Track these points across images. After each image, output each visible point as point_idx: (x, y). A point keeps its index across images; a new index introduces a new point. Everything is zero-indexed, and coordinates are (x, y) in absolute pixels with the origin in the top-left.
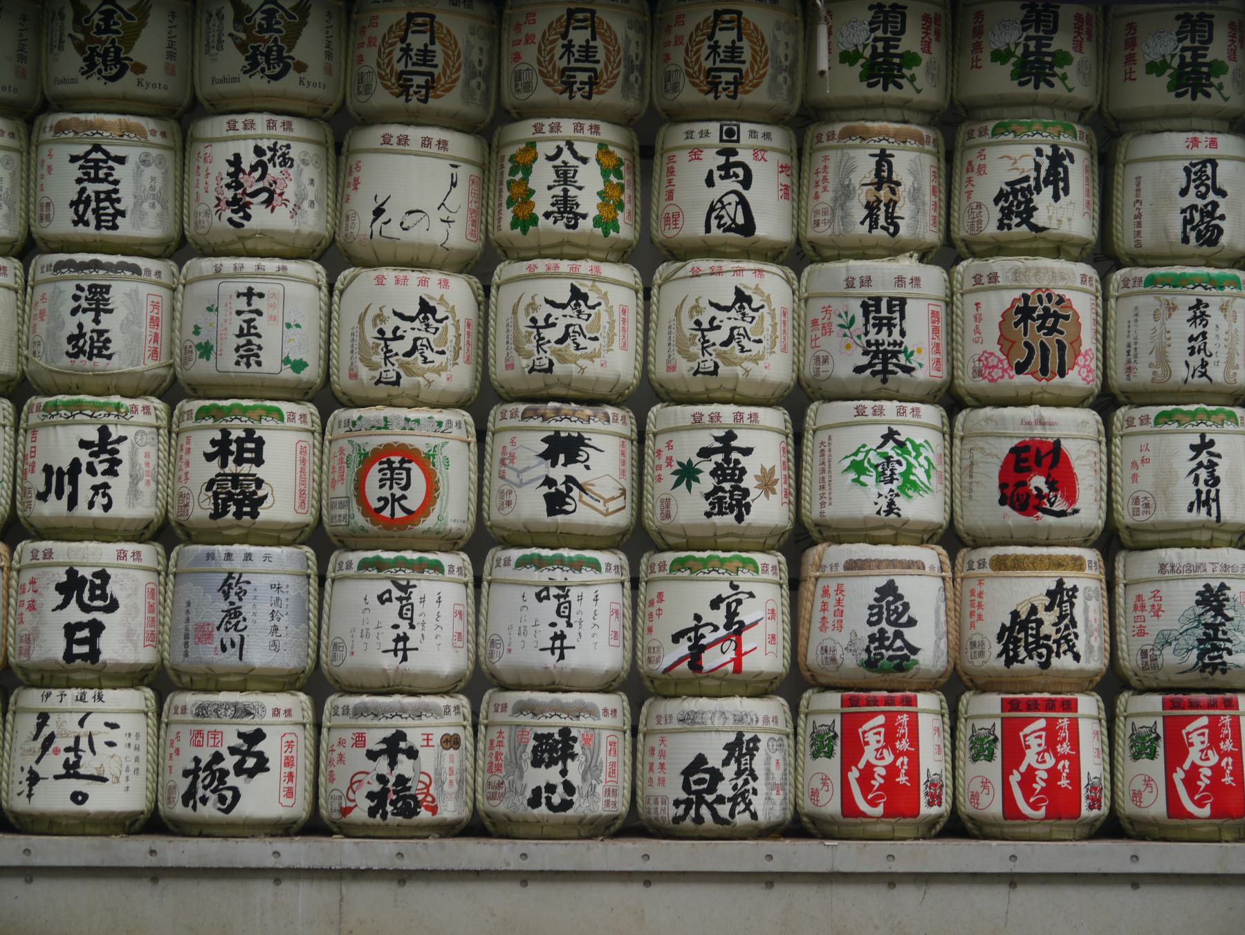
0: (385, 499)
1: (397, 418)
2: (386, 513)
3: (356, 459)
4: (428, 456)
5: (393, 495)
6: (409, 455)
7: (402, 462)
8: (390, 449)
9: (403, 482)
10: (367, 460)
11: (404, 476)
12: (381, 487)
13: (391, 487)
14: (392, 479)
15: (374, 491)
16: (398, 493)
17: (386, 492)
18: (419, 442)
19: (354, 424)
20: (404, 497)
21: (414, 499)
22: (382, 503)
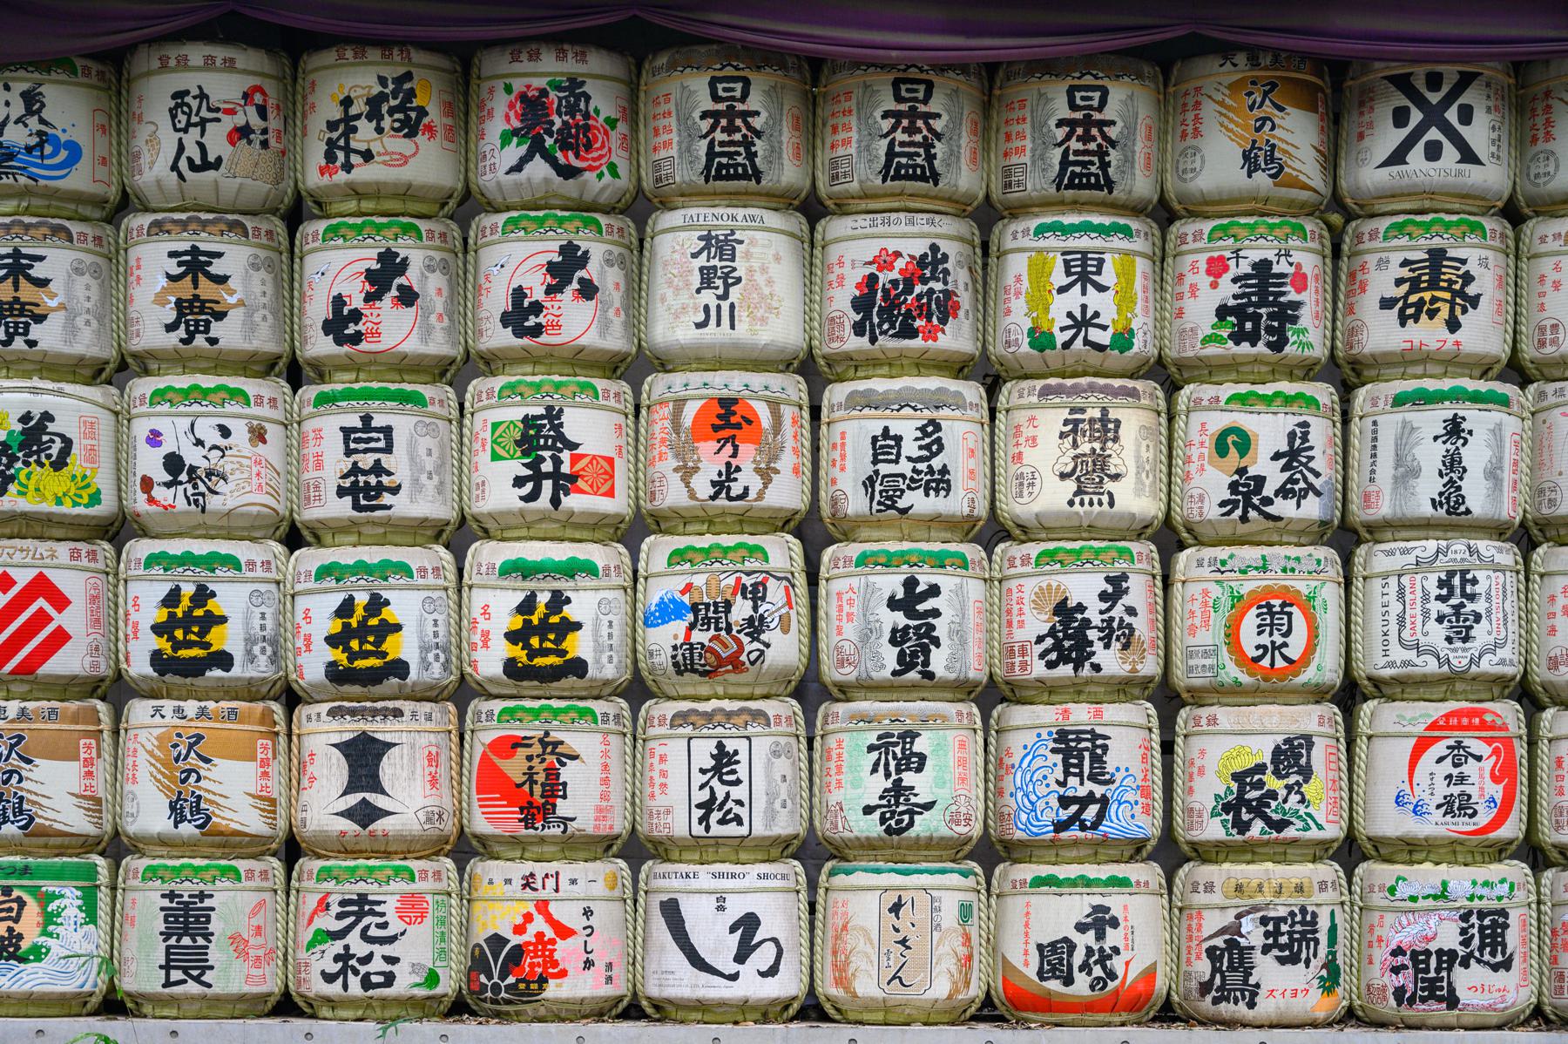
0: (1265, 647)
1: (1276, 557)
2: (1266, 662)
3: (1226, 602)
4: (1309, 599)
5: (1273, 643)
6: (1290, 600)
7: (1283, 605)
8: (1270, 592)
9: (1285, 628)
10: (1240, 605)
11: (1285, 621)
12: (1259, 633)
13: (1271, 634)
14: (1271, 625)
15: (1250, 639)
16: (1279, 640)
17: (1265, 639)
18: (1303, 587)
19: (1223, 563)
20: (1285, 645)
21: (1295, 650)
22: (1261, 651)
